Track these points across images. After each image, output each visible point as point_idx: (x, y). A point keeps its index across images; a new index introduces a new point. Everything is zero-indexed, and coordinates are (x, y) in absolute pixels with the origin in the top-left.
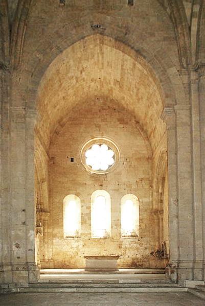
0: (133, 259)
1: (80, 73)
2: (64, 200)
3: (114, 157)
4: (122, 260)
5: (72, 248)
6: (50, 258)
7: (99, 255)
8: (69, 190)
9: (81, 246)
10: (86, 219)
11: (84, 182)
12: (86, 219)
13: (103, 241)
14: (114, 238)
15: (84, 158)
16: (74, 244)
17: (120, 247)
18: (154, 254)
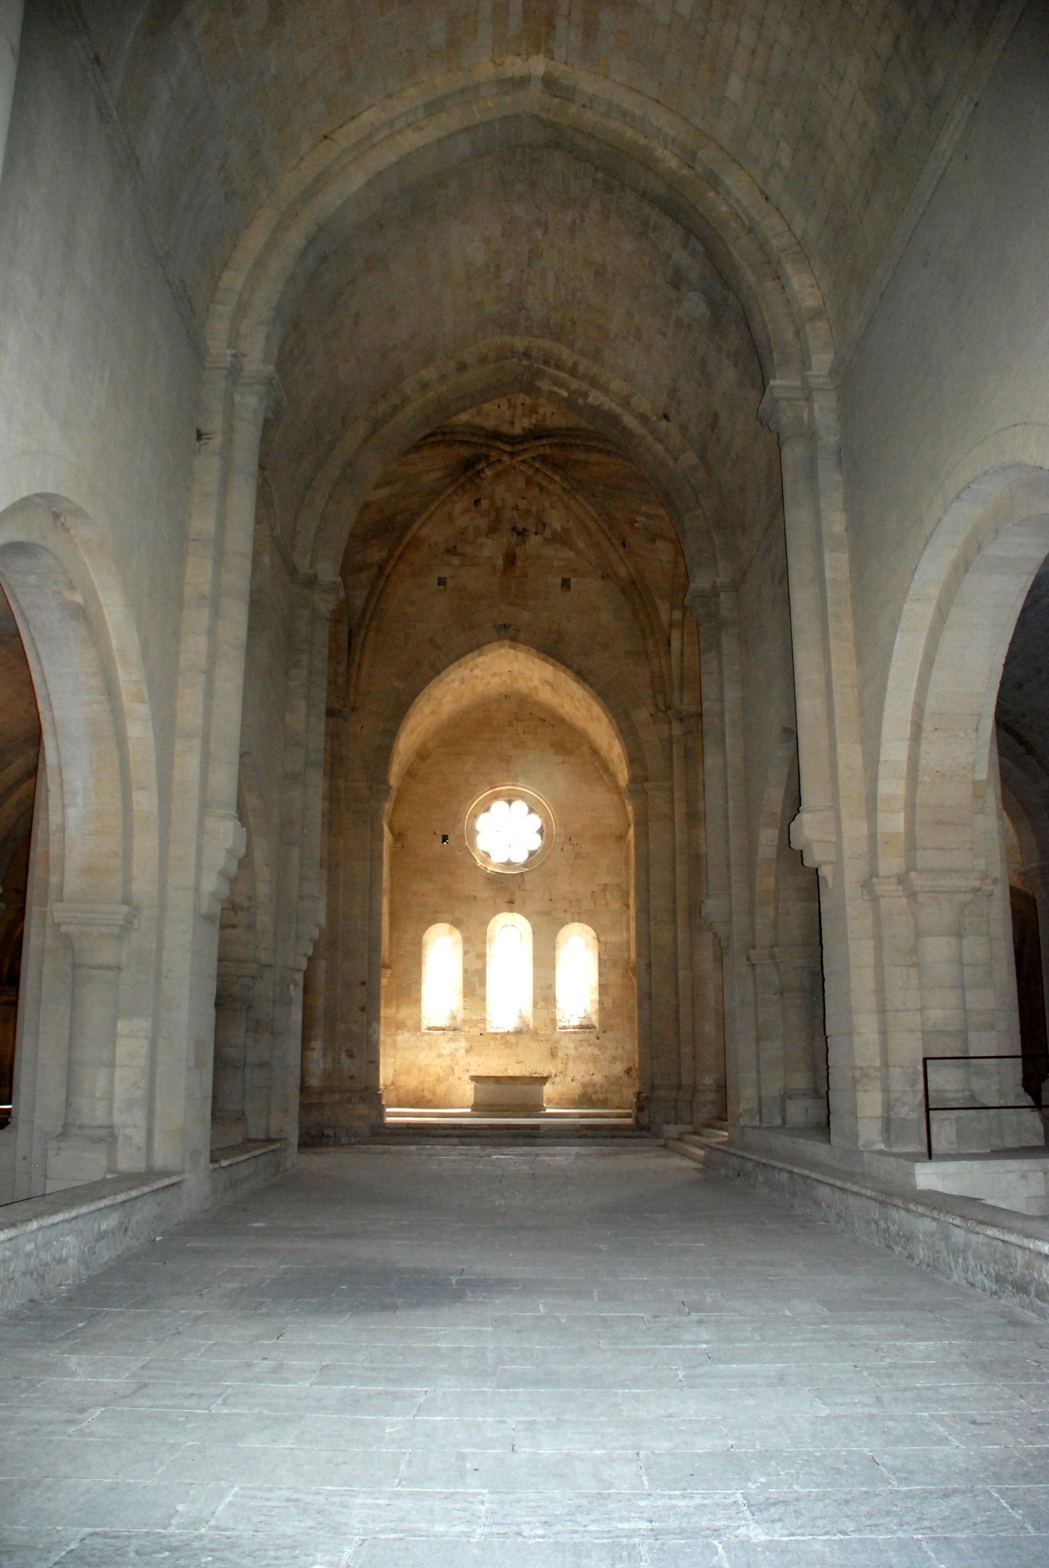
0: (585, 1086)
2: (425, 936)
3: (541, 832)
4: (559, 1088)
5: (440, 1056)
6: (389, 1082)
7: (505, 1074)
8: (437, 912)
9: (462, 1052)
10: (474, 983)
11: (472, 893)
12: (474, 983)
13: (512, 1039)
14: (539, 1030)
15: (473, 833)
16: (446, 1047)
17: (553, 1054)
18: (634, 1073)
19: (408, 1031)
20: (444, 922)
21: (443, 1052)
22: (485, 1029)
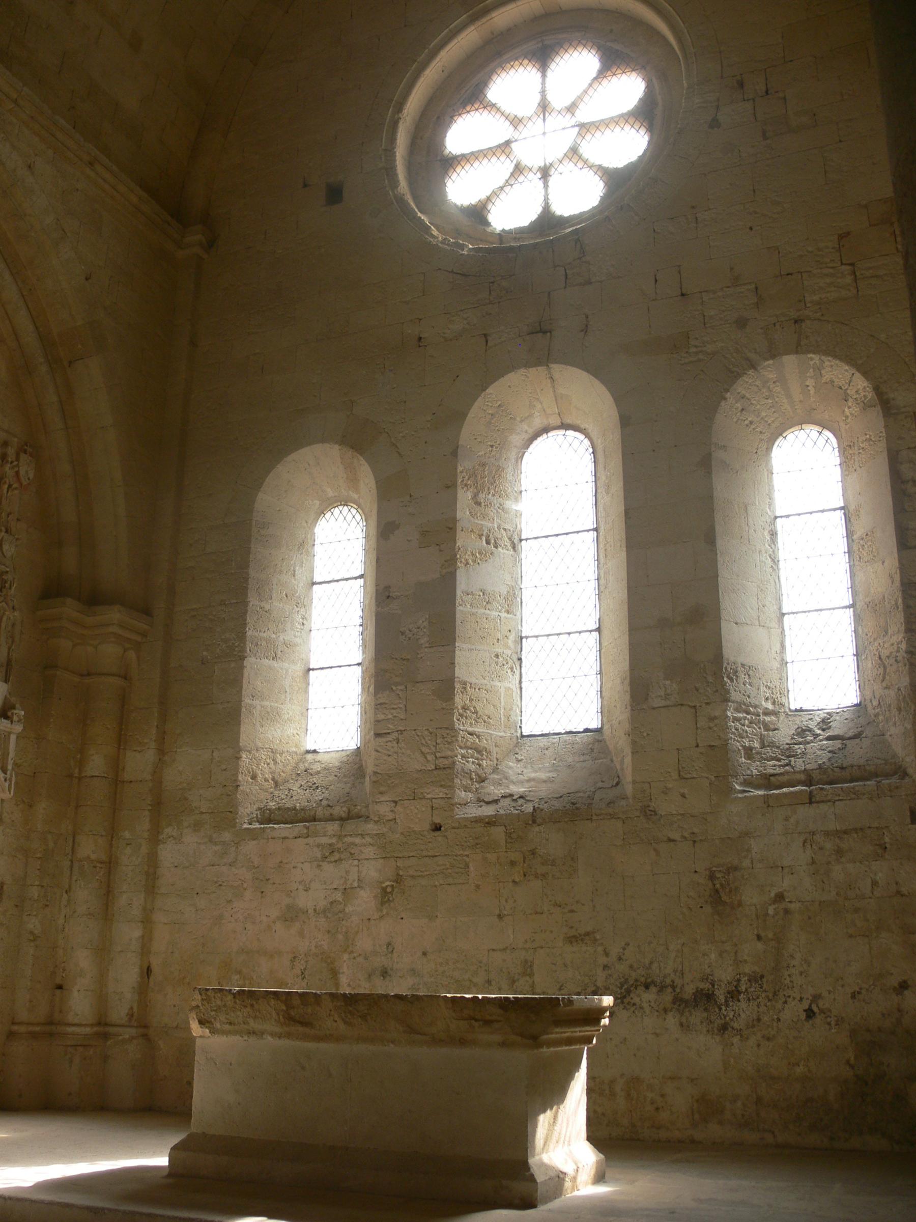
9: (365, 900)
13: (552, 842)
16: (312, 882)
17: (720, 894)
19: (197, 826)
21: (304, 901)
22: (450, 804)
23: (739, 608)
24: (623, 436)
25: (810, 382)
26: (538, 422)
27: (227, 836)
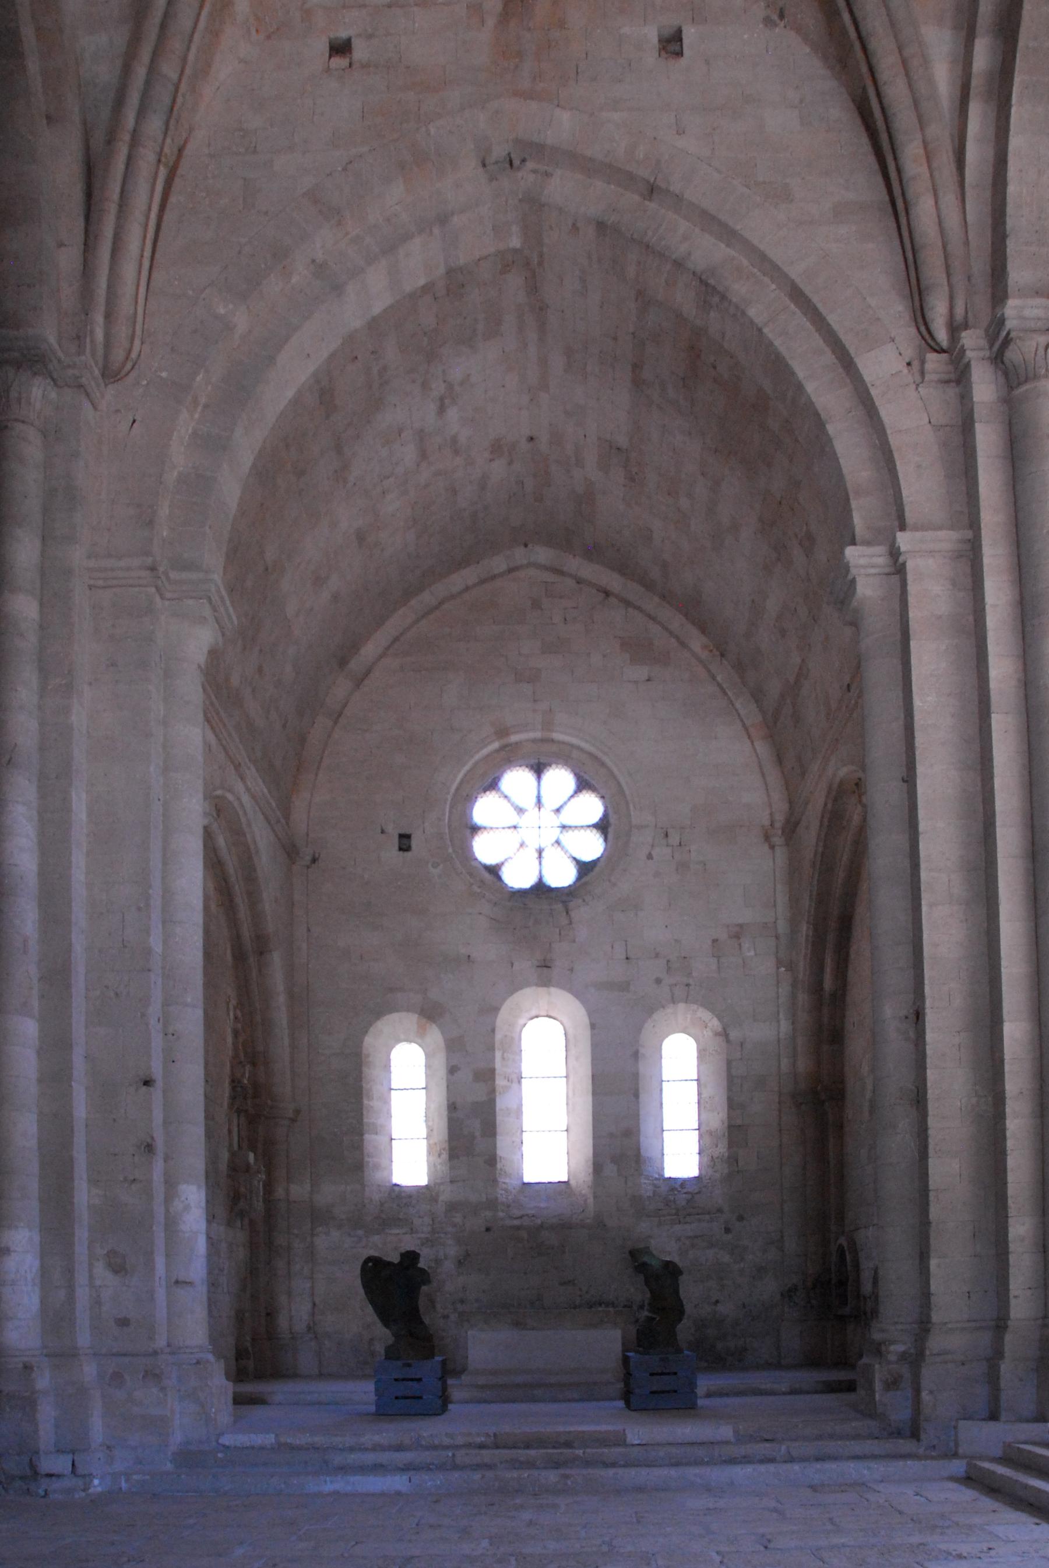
1: (433, 407)
2: (368, 1040)
8: (391, 990)
20: (408, 1010)
23: (647, 1128)
24: (593, 1036)
25: (689, 1016)
26: (534, 1013)
27: (360, 1232)
